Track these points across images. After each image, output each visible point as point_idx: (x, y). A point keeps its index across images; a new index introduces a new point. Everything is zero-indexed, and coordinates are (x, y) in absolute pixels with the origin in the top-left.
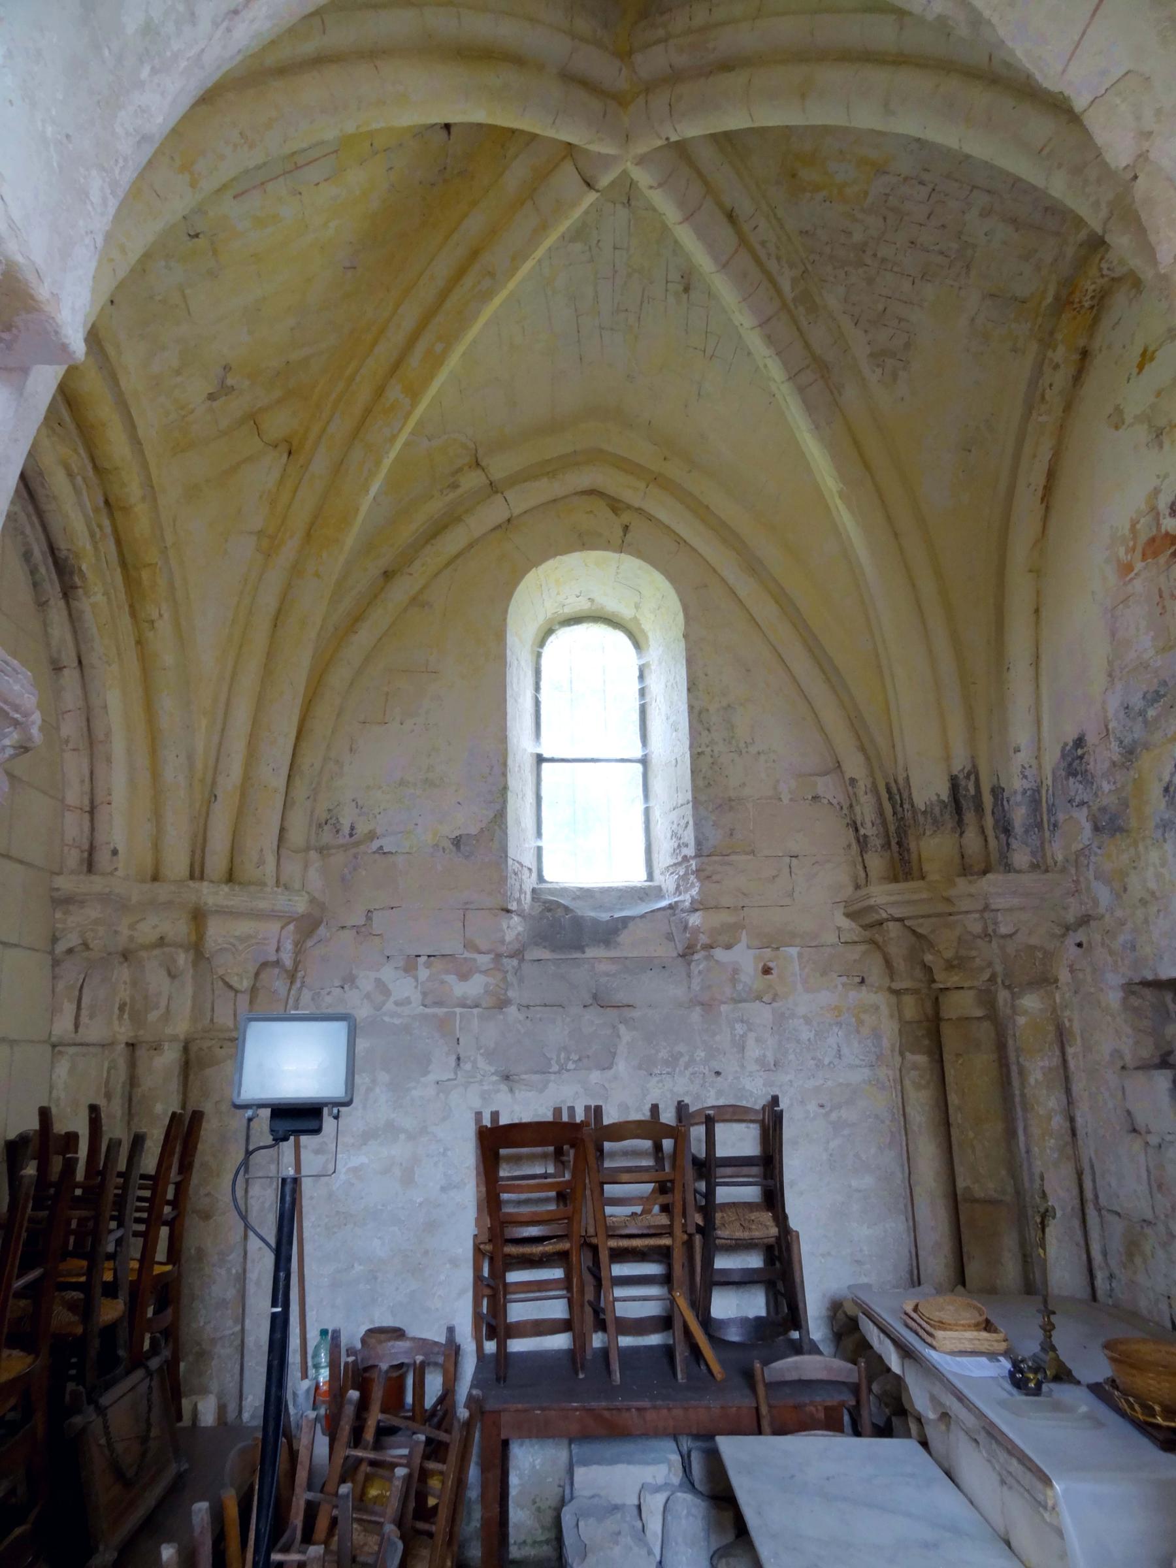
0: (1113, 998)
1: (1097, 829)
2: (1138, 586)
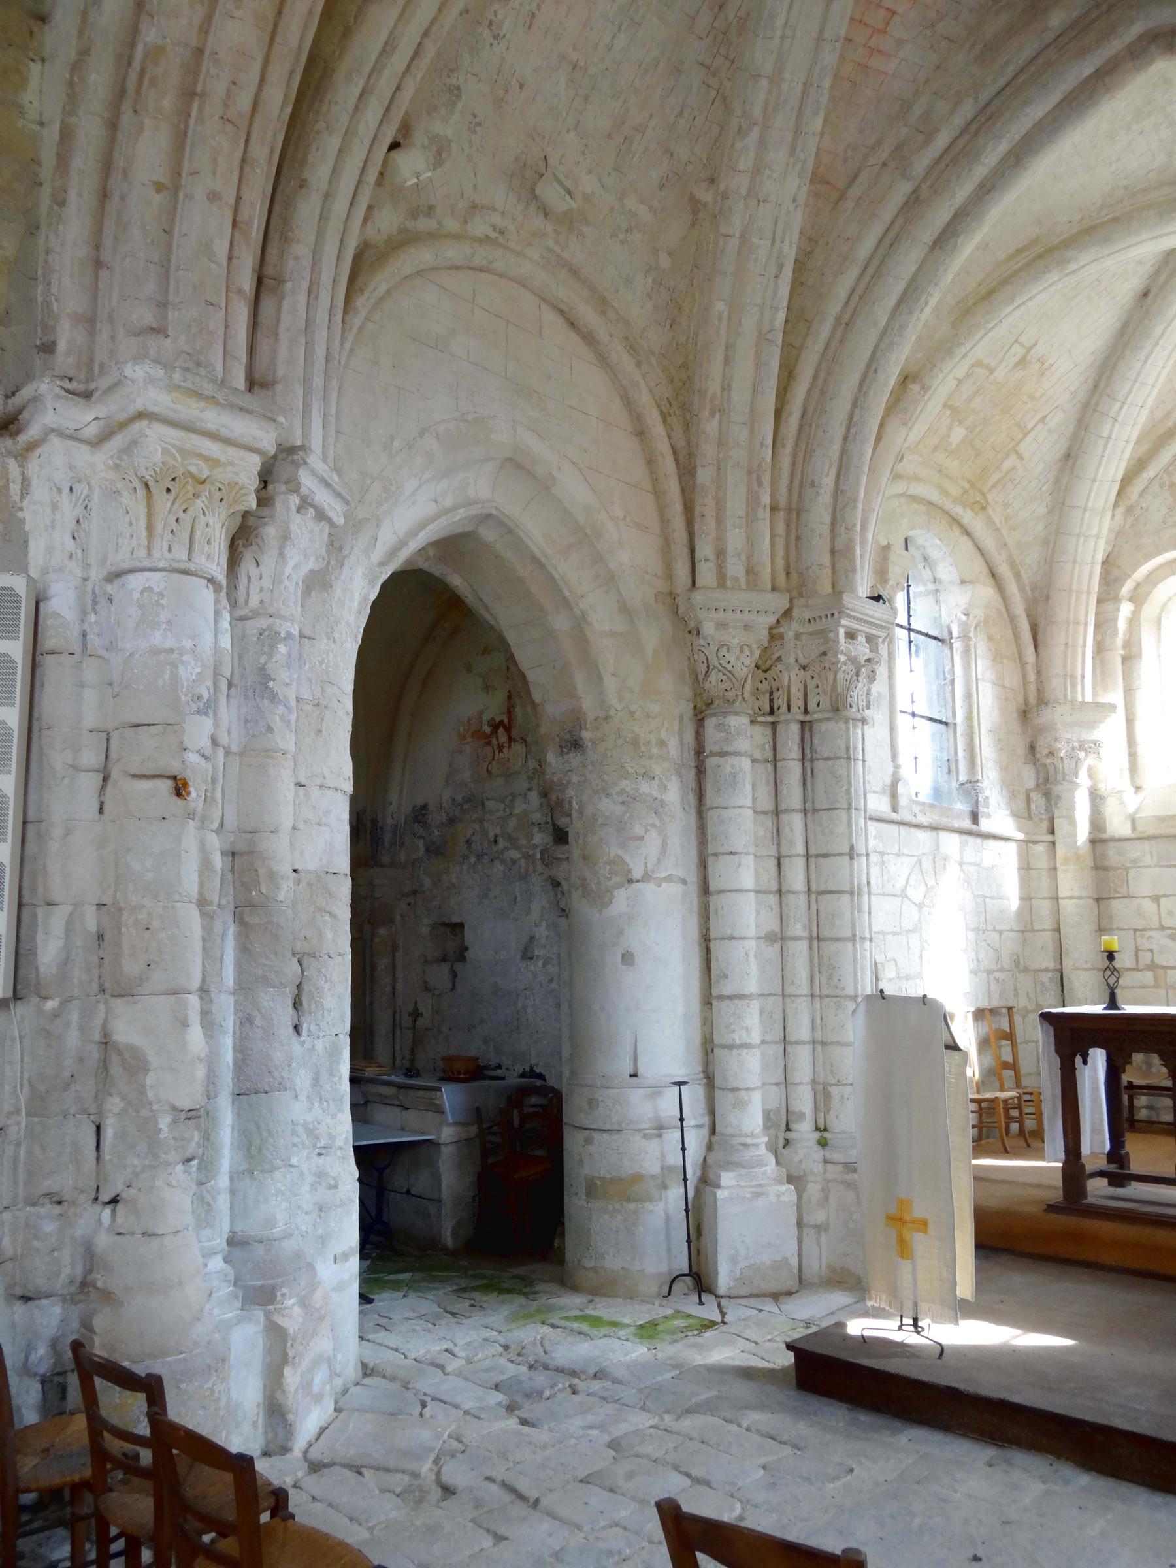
0: (425, 931)
1: (428, 850)
2: (468, 748)
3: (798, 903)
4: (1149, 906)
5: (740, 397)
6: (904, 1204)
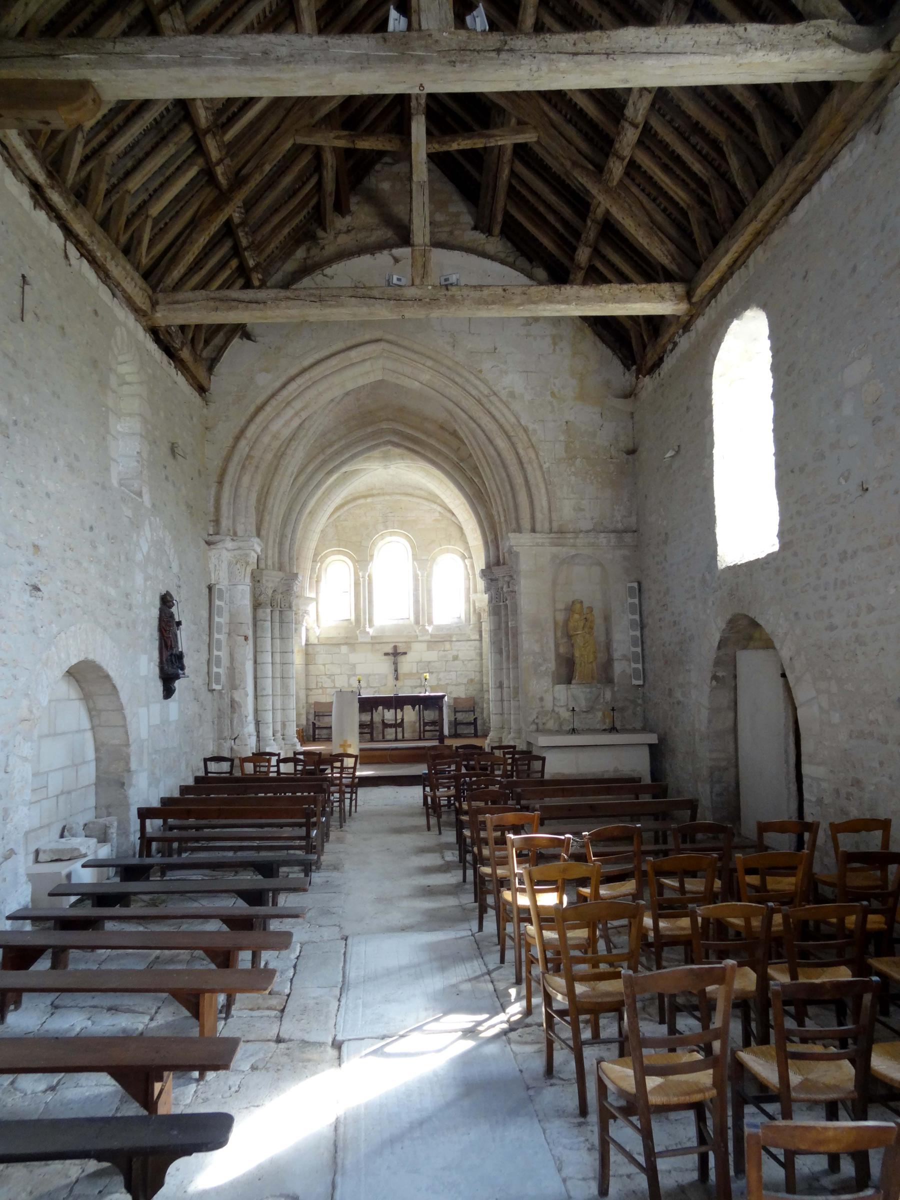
3: (278, 667)
4: (322, 667)
5: (276, 509)
6: (345, 741)
